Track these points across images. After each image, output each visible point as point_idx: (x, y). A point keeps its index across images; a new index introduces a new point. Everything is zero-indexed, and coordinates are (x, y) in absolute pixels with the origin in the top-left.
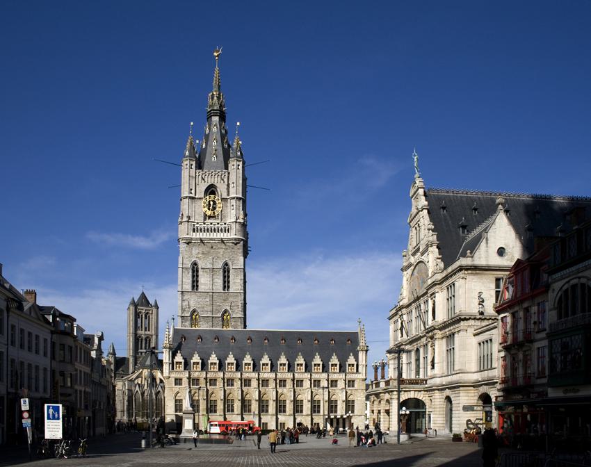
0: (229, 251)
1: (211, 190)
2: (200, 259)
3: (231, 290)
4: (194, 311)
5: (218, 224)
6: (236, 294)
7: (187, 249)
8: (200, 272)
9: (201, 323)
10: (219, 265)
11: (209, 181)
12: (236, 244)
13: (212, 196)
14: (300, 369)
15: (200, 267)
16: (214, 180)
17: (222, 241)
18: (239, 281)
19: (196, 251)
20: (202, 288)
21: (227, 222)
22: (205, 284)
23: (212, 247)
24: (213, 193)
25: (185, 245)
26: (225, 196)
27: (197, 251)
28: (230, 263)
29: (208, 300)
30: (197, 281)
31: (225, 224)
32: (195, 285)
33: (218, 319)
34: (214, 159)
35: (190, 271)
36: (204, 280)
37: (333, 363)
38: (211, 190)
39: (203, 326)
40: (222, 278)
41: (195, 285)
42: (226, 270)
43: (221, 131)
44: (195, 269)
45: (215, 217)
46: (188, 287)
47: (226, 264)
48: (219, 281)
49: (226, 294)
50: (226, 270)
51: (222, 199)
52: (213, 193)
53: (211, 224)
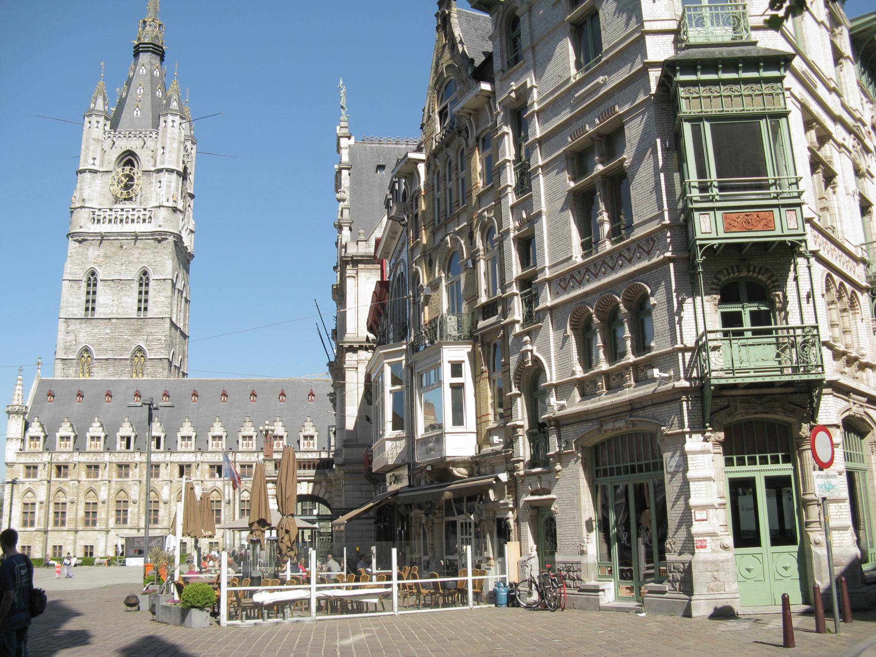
0: (149, 251)
1: (129, 159)
2: (100, 266)
3: (150, 314)
5: (133, 210)
6: (157, 321)
7: (80, 250)
9: (94, 369)
10: (134, 274)
11: (123, 145)
12: (159, 241)
13: (128, 168)
14: (248, 445)
16: (134, 144)
17: (136, 237)
18: (162, 299)
19: (93, 252)
20: (100, 312)
22: (105, 305)
23: (121, 247)
24: (130, 163)
25: (77, 244)
27: (96, 253)
28: (150, 271)
29: (108, 331)
31: (145, 209)
32: (90, 305)
33: (123, 362)
34: (135, 113)
35: (84, 285)
36: (104, 297)
37: (307, 433)
39: (100, 374)
41: (90, 305)
42: (144, 278)
43: (152, 73)
44: (92, 279)
45: (131, 199)
47: (145, 273)
48: (129, 302)
49: (140, 322)
50: (144, 278)
52: (130, 163)
53: (122, 210)
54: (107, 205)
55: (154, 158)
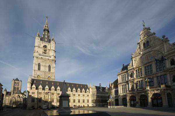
4: (38, 75)
8: (41, 66)
10: (48, 65)
15: (41, 64)
21: (50, 55)
22: (43, 69)
26: (50, 49)
30: (40, 68)
32: (39, 69)
36: (42, 68)
38: (45, 47)
40: (48, 68)
41: (39, 69)
44: (39, 65)
46: (37, 69)
51: (49, 50)
54: (42, 53)
55: (50, 48)
